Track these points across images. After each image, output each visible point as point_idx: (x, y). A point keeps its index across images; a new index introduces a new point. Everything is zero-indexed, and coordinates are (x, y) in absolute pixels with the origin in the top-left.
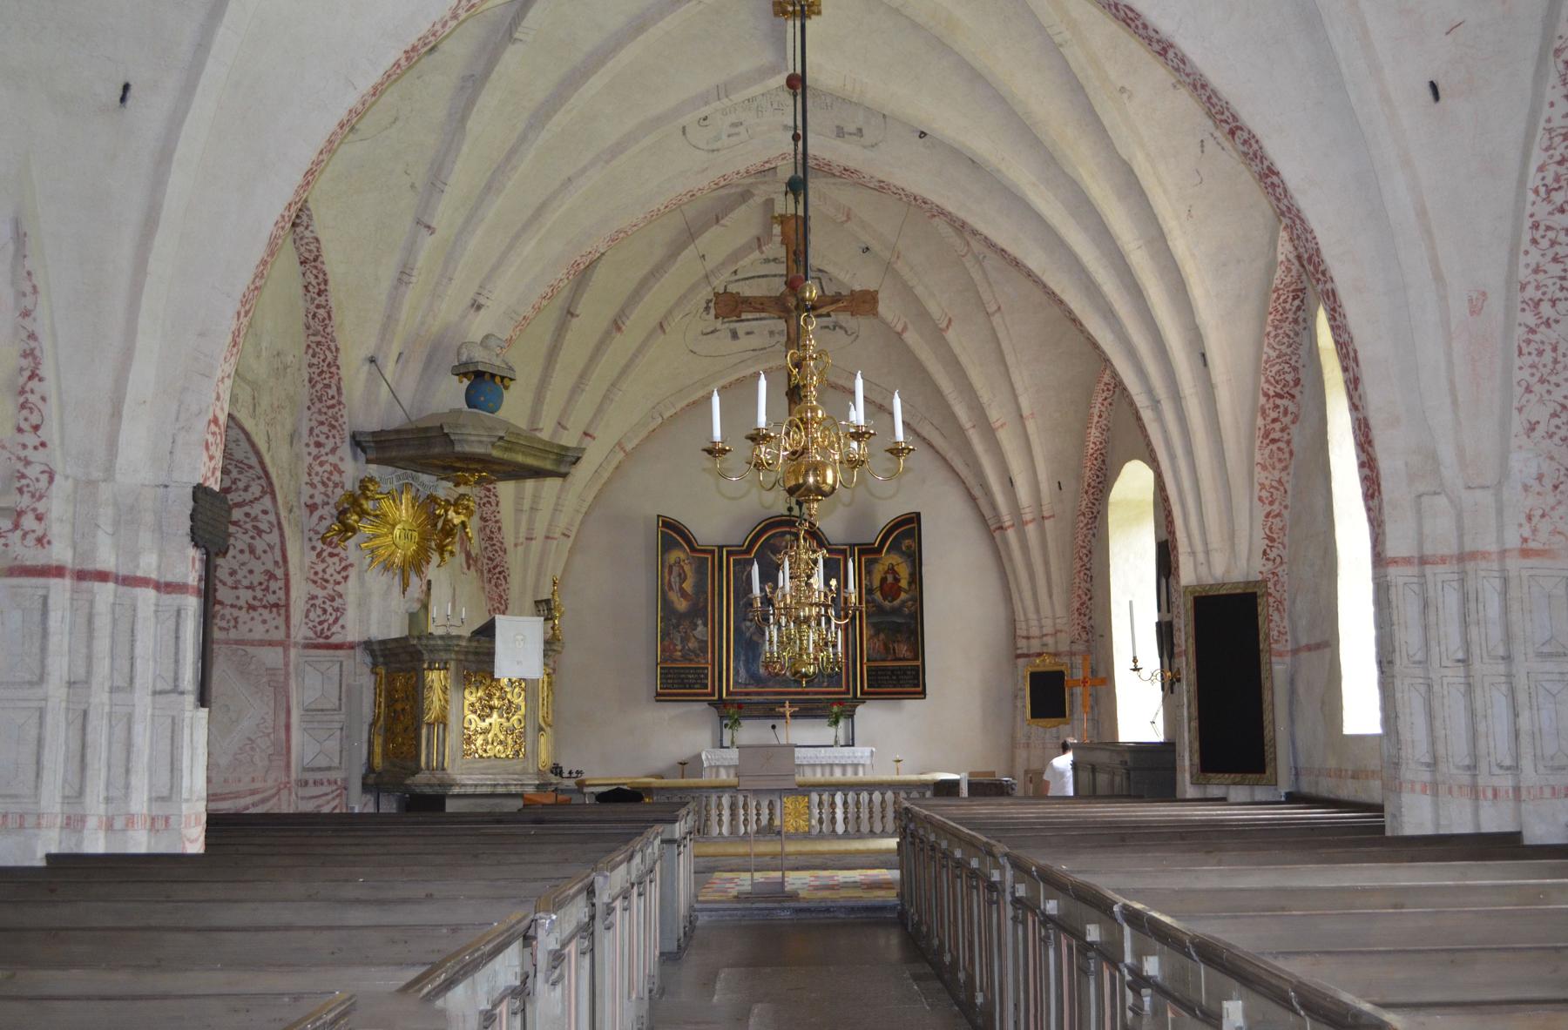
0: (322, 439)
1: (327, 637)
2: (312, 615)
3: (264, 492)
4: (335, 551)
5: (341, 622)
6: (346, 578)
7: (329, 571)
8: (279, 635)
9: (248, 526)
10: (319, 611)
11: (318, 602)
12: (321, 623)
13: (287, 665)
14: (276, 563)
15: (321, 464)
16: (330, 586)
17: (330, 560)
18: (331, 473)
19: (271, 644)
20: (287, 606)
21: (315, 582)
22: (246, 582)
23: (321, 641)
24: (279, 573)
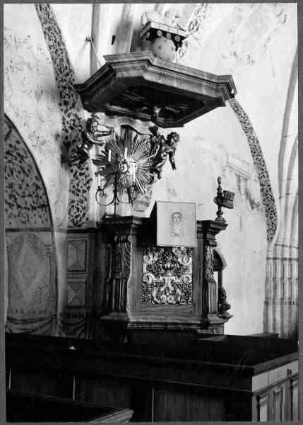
0: (67, 99)
1: (80, 226)
2: (72, 213)
3: (10, 127)
4: (83, 171)
5: (86, 216)
6: (89, 188)
7: (81, 184)
8: (48, 224)
9: (15, 154)
10: (75, 210)
11: (75, 204)
12: (77, 217)
13: (53, 243)
14: (36, 177)
15: (69, 116)
16: (80, 194)
17: (80, 178)
18: (74, 121)
19: (45, 230)
20: (49, 205)
21: (73, 192)
22: (27, 193)
23: (77, 228)
24: (40, 184)
